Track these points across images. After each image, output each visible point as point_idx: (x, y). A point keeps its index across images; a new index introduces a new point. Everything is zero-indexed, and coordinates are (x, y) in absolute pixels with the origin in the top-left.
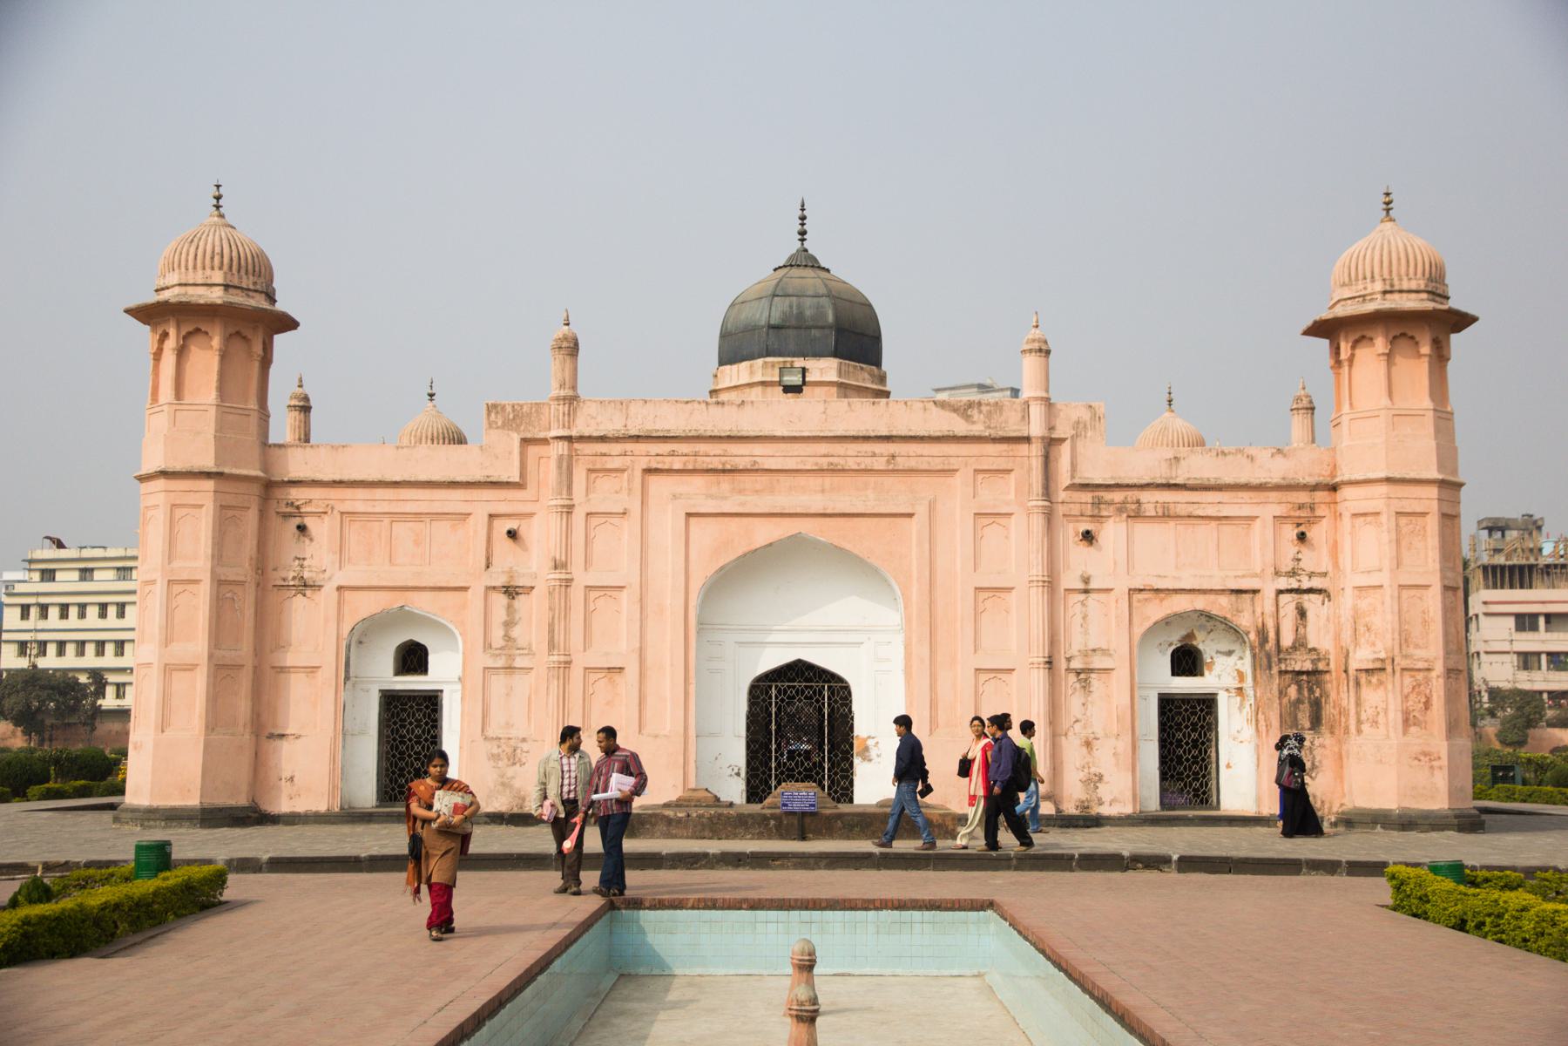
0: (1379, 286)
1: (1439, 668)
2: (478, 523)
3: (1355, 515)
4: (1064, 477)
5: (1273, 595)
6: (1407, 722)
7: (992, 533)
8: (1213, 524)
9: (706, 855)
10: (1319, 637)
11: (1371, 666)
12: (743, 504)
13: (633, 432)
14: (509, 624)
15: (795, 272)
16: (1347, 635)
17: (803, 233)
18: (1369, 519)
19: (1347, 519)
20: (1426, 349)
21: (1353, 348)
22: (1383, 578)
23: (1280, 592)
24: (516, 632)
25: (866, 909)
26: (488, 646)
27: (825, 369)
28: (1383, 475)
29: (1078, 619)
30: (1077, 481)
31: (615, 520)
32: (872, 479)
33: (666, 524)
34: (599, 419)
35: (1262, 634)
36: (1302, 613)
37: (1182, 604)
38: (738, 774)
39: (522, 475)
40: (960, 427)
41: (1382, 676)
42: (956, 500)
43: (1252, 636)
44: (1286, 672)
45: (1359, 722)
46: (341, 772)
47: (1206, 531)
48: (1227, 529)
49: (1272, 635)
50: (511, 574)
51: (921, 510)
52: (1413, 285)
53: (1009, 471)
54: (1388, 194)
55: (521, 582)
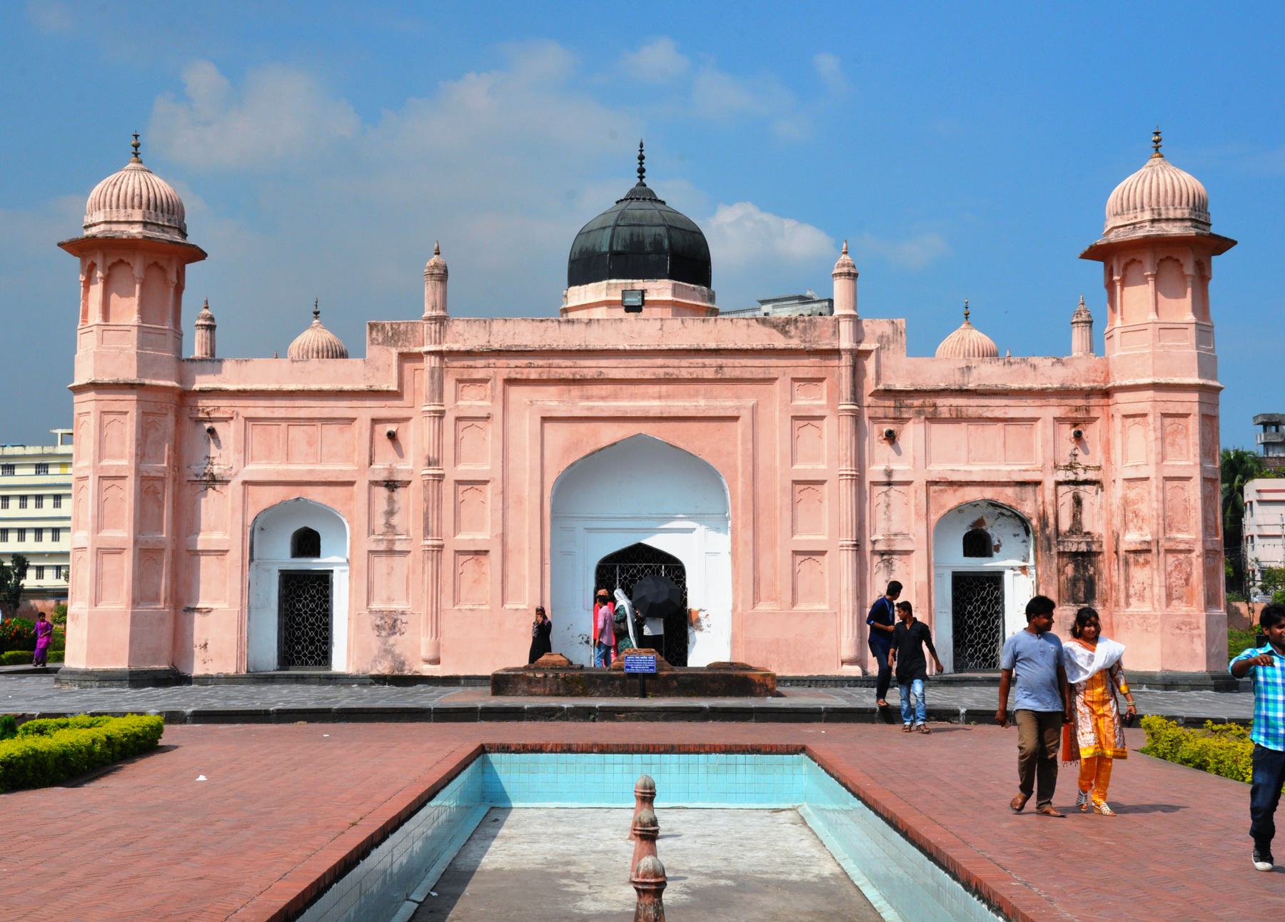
0: (1147, 216)
1: (1198, 549)
2: (363, 426)
3: (1126, 416)
4: (870, 385)
5: (1052, 486)
6: (1169, 597)
7: (808, 432)
8: (1000, 425)
9: (561, 709)
11: (1139, 547)
12: (590, 408)
13: (496, 346)
14: (390, 513)
15: (635, 204)
16: (1117, 521)
17: (641, 171)
18: (1138, 419)
19: (1118, 421)
20: (1189, 269)
21: (1125, 269)
22: (1149, 471)
23: (1058, 483)
24: (395, 520)
25: (698, 753)
26: (371, 532)
27: (660, 289)
29: (882, 508)
30: (881, 387)
33: (525, 427)
34: (466, 335)
35: (1043, 519)
36: (1078, 502)
37: (973, 494)
38: (587, 642)
39: (401, 384)
40: (780, 342)
41: (1149, 556)
42: (778, 403)
43: (1034, 522)
44: (1064, 553)
45: (1128, 596)
46: (247, 641)
48: (1012, 429)
49: (1051, 521)
50: (391, 471)
51: (746, 416)
52: (1179, 214)
53: (821, 380)
54: (1157, 134)
55: (399, 477)
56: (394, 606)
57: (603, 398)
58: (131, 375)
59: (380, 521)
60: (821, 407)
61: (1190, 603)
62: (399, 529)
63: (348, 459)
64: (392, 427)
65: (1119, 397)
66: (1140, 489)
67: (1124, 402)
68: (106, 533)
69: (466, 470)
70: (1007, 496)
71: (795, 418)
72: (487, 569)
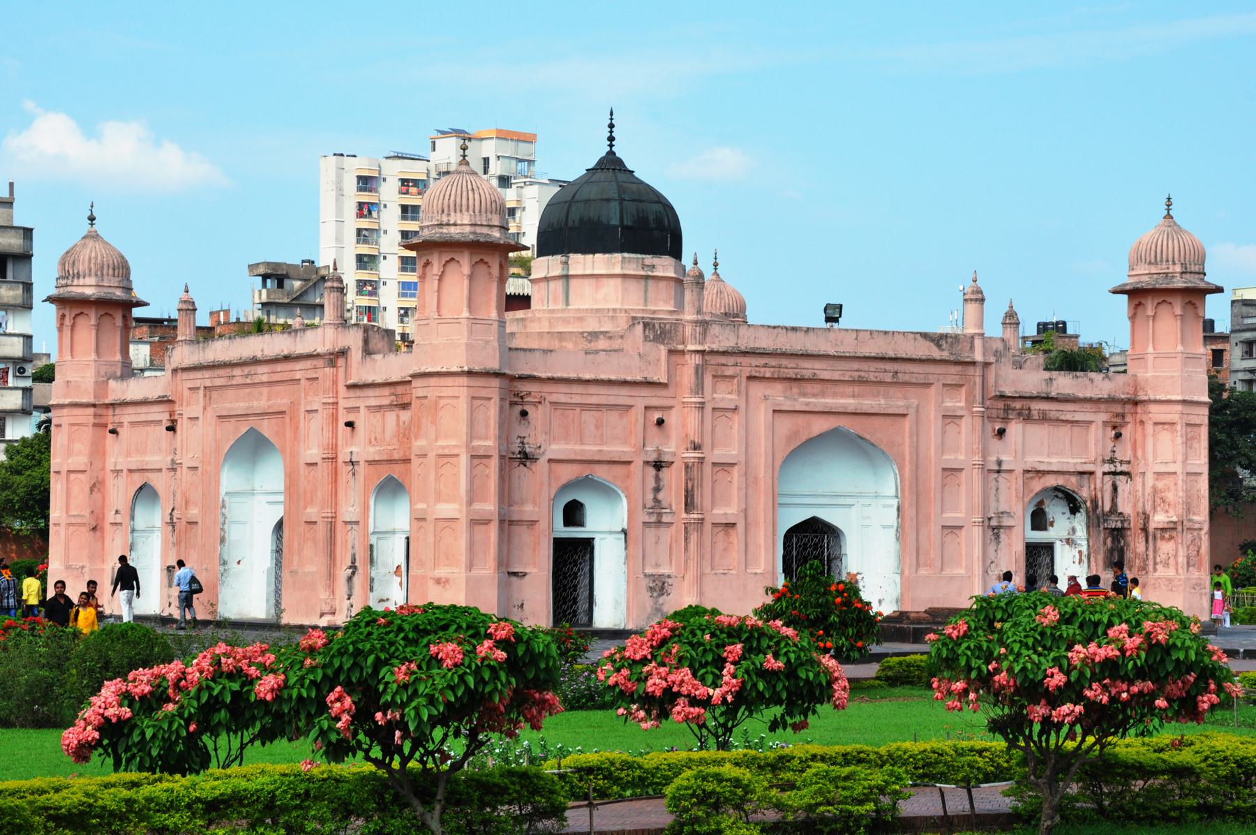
2: (638, 411)
3: (1156, 424)
7: (951, 429)
10: (1125, 507)
12: (807, 404)
13: (743, 348)
14: (657, 489)
17: (611, 139)
19: (1149, 428)
22: (1177, 467)
23: (1104, 474)
24: (661, 496)
28: (1179, 398)
29: (994, 491)
32: (882, 389)
33: (762, 416)
36: (1115, 488)
40: (936, 354)
41: (1174, 534)
45: (1155, 564)
47: (1064, 431)
51: (912, 412)
53: (961, 386)
55: (666, 458)
56: (661, 571)
57: (814, 396)
58: (494, 365)
59: (650, 496)
60: (961, 408)
61: (1199, 569)
62: (664, 504)
63: (625, 441)
64: (657, 415)
65: (1153, 408)
66: (1168, 481)
67: (1156, 412)
68: (477, 506)
69: (719, 454)
70: (1071, 483)
71: (944, 416)
72: (734, 539)
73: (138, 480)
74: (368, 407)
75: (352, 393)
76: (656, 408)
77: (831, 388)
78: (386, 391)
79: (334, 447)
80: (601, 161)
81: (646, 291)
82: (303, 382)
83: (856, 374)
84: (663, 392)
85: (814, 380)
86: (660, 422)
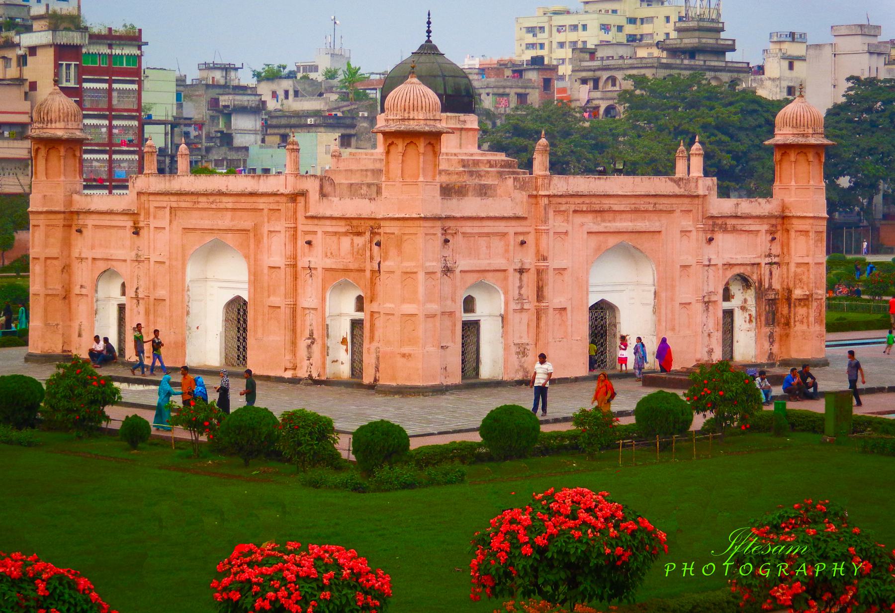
0: (811, 131)
3: (796, 231)
12: (606, 227)
13: (571, 192)
14: (520, 287)
17: (429, 32)
19: (793, 234)
31: (562, 236)
32: (647, 215)
47: (744, 238)
55: (527, 266)
61: (820, 325)
62: (525, 297)
64: (521, 238)
65: (795, 221)
70: (746, 271)
71: (682, 231)
73: (102, 266)
74: (325, 233)
75: (310, 221)
76: (521, 233)
77: (619, 217)
78: (343, 223)
79: (295, 258)
80: (422, 47)
81: (461, 139)
82: (266, 211)
83: (633, 206)
84: (524, 223)
85: (610, 211)
86: (523, 243)
